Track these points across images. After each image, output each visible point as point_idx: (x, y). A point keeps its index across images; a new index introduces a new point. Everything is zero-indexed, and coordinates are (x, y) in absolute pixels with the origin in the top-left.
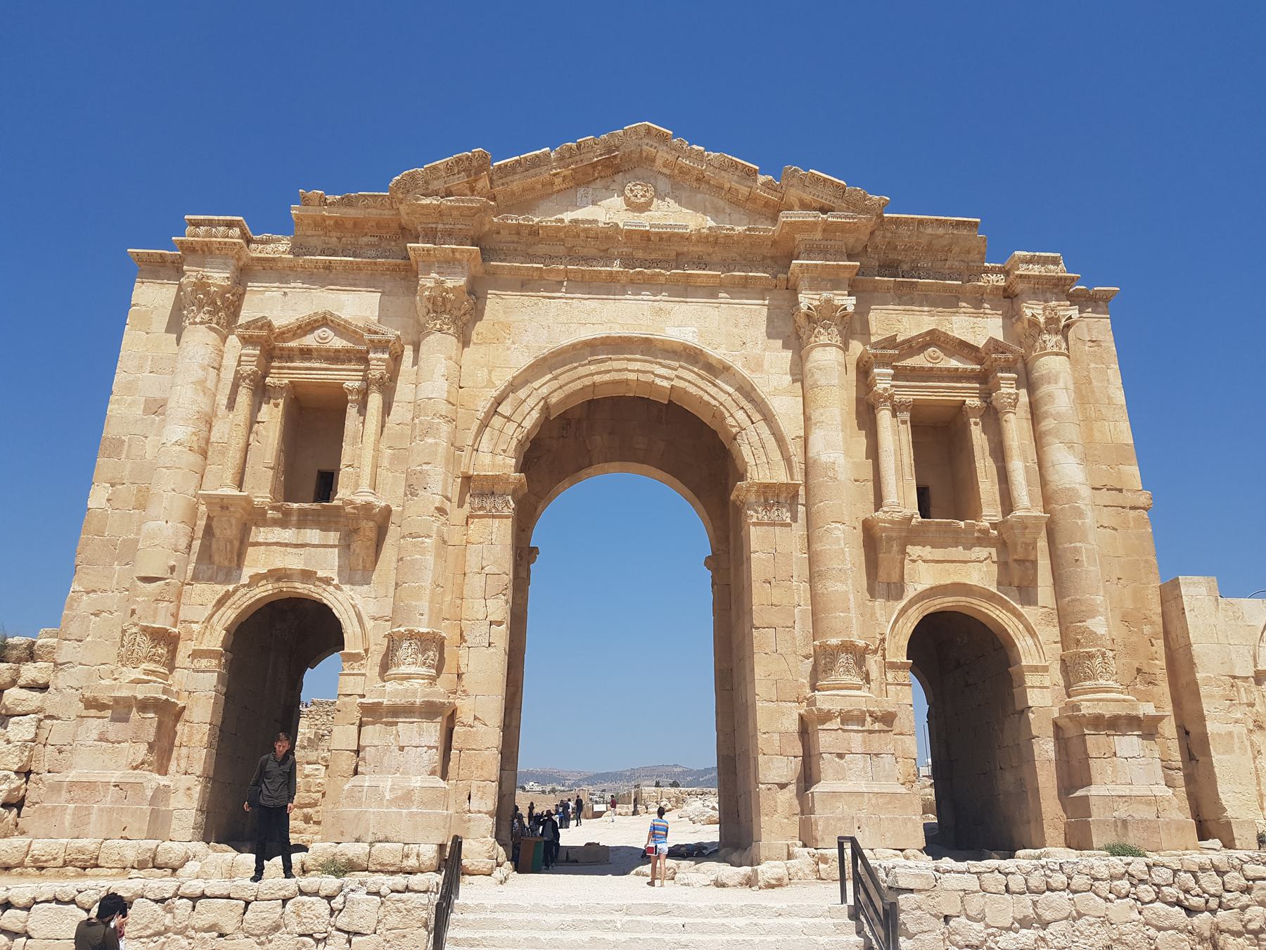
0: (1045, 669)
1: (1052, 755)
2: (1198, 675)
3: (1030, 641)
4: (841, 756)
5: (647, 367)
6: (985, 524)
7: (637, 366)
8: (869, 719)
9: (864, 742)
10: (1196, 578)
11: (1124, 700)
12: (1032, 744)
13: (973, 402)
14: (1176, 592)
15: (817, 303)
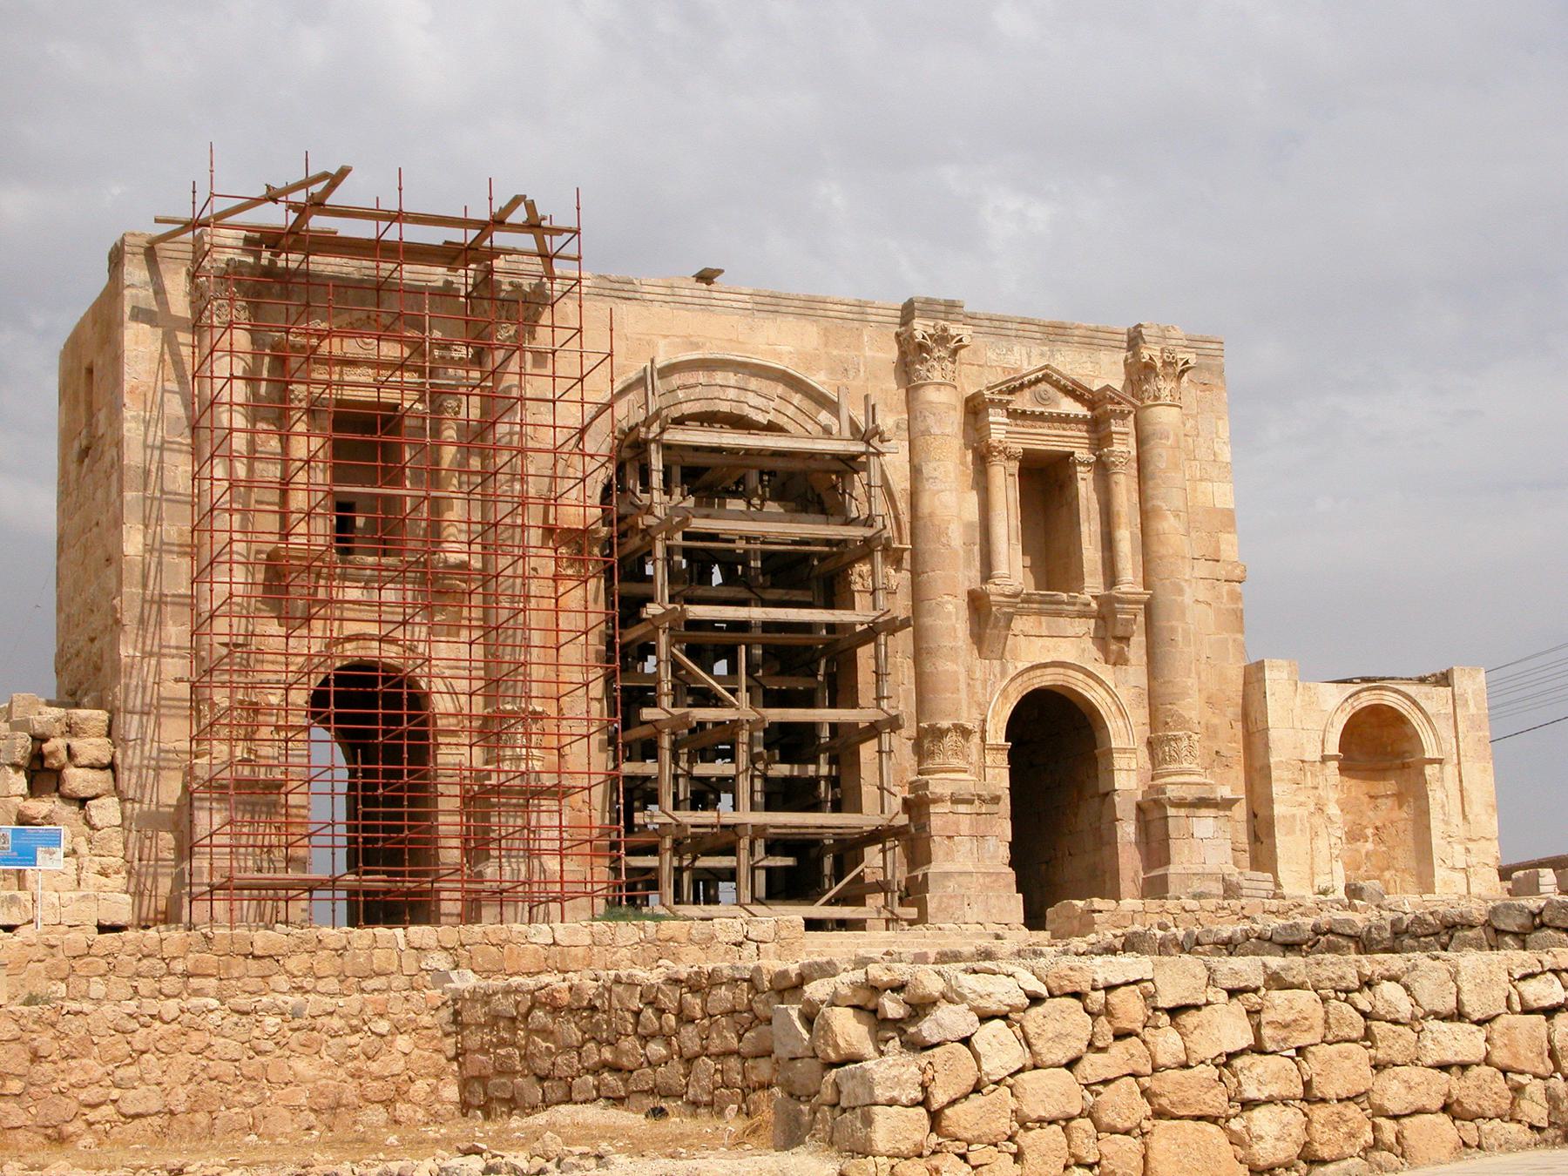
0: (1133, 751)
1: (1133, 837)
2: (1272, 760)
3: (1120, 723)
4: (949, 837)
5: (743, 396)
6: (1086, 597)
7: (732, 394)
8: (977, 802)
9: (972, 824)
10: (1280, 662)
11: (1205, 784)
12: (1115, 827)
13: (1082, 454)
14: (1260, 675)
15: (932, 331)
